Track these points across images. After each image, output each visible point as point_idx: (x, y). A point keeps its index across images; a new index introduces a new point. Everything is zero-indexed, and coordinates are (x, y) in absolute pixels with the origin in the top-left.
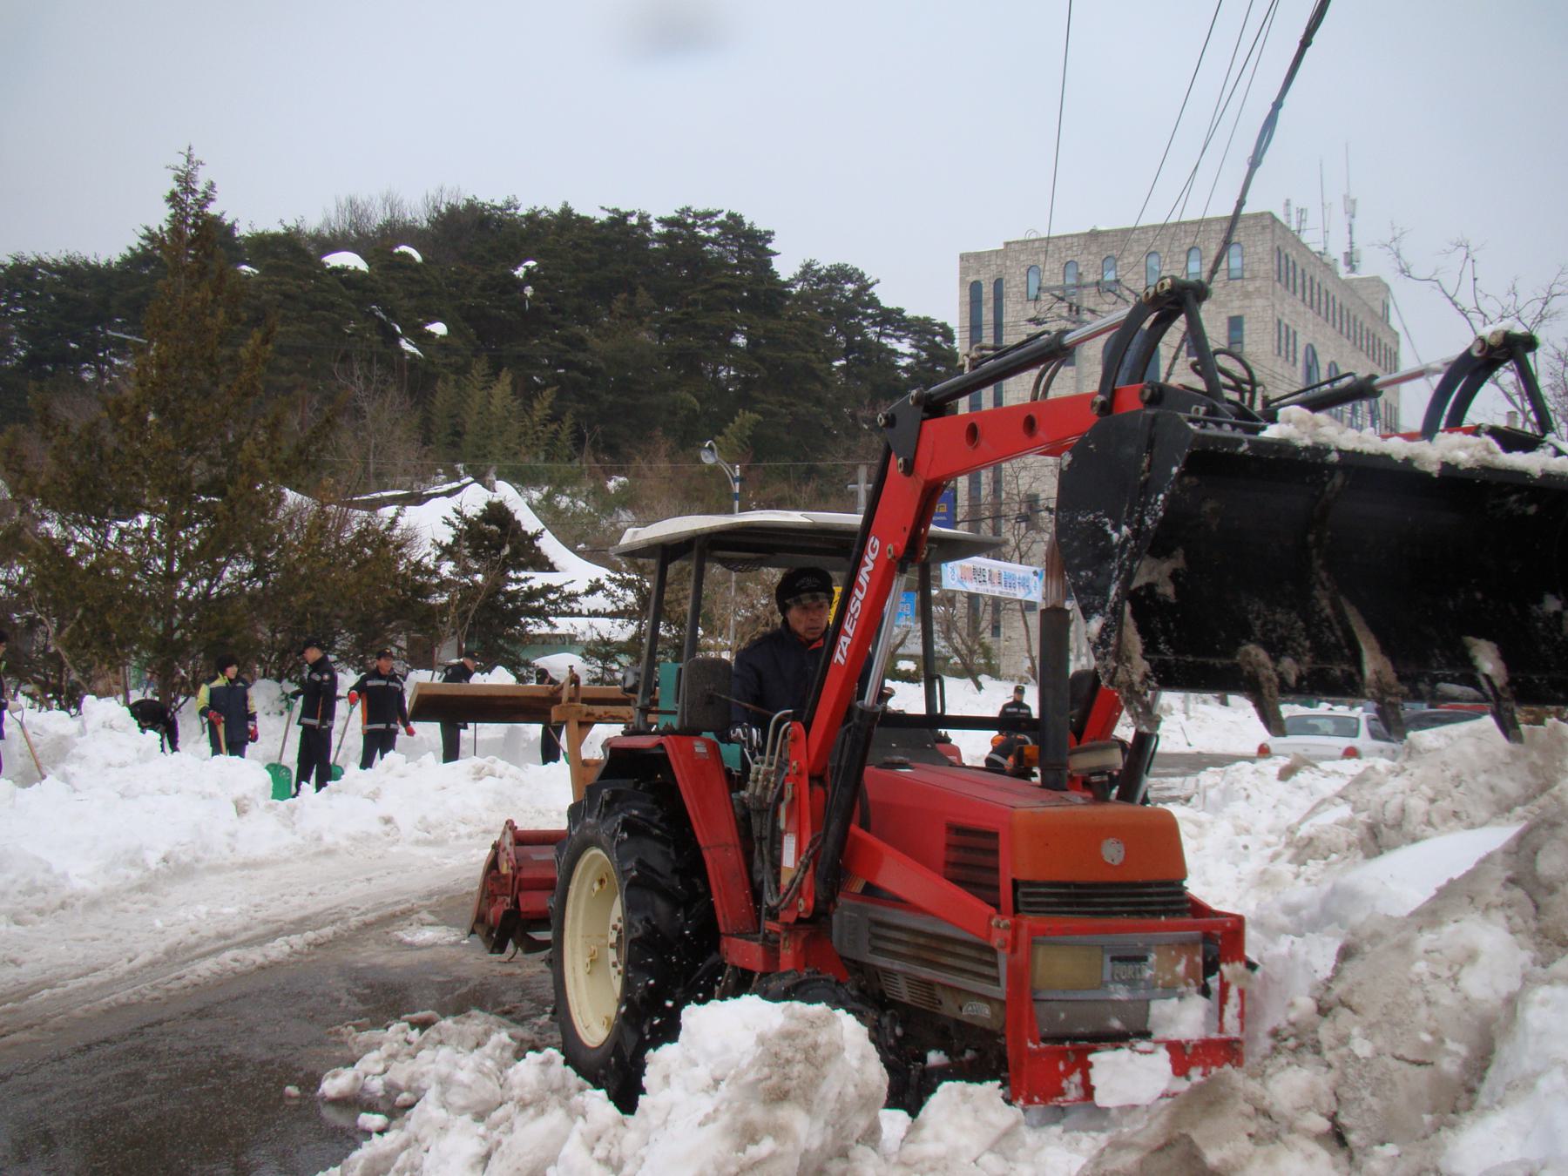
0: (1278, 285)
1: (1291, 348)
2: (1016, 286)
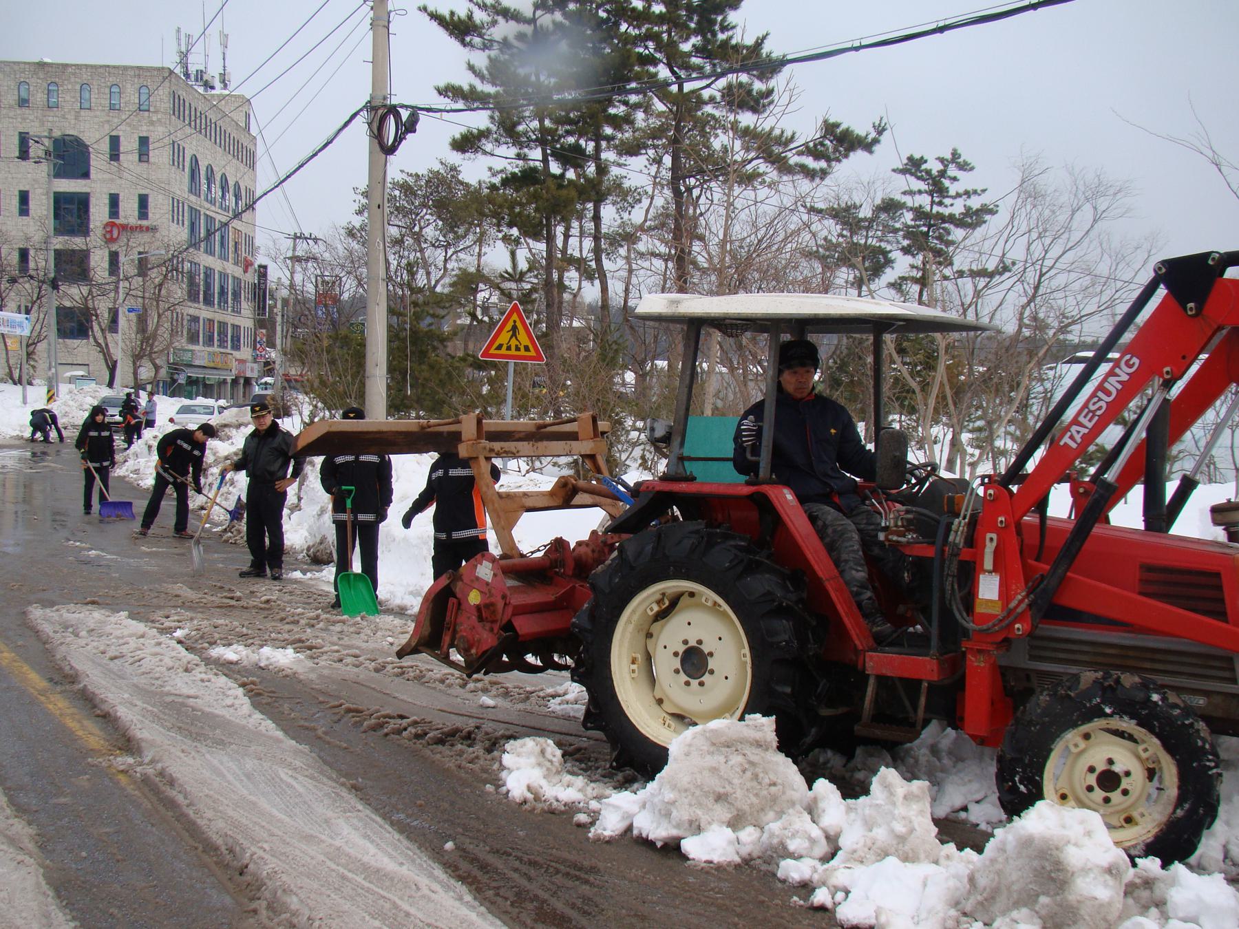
0: (173, 117)
1: (181, 159)
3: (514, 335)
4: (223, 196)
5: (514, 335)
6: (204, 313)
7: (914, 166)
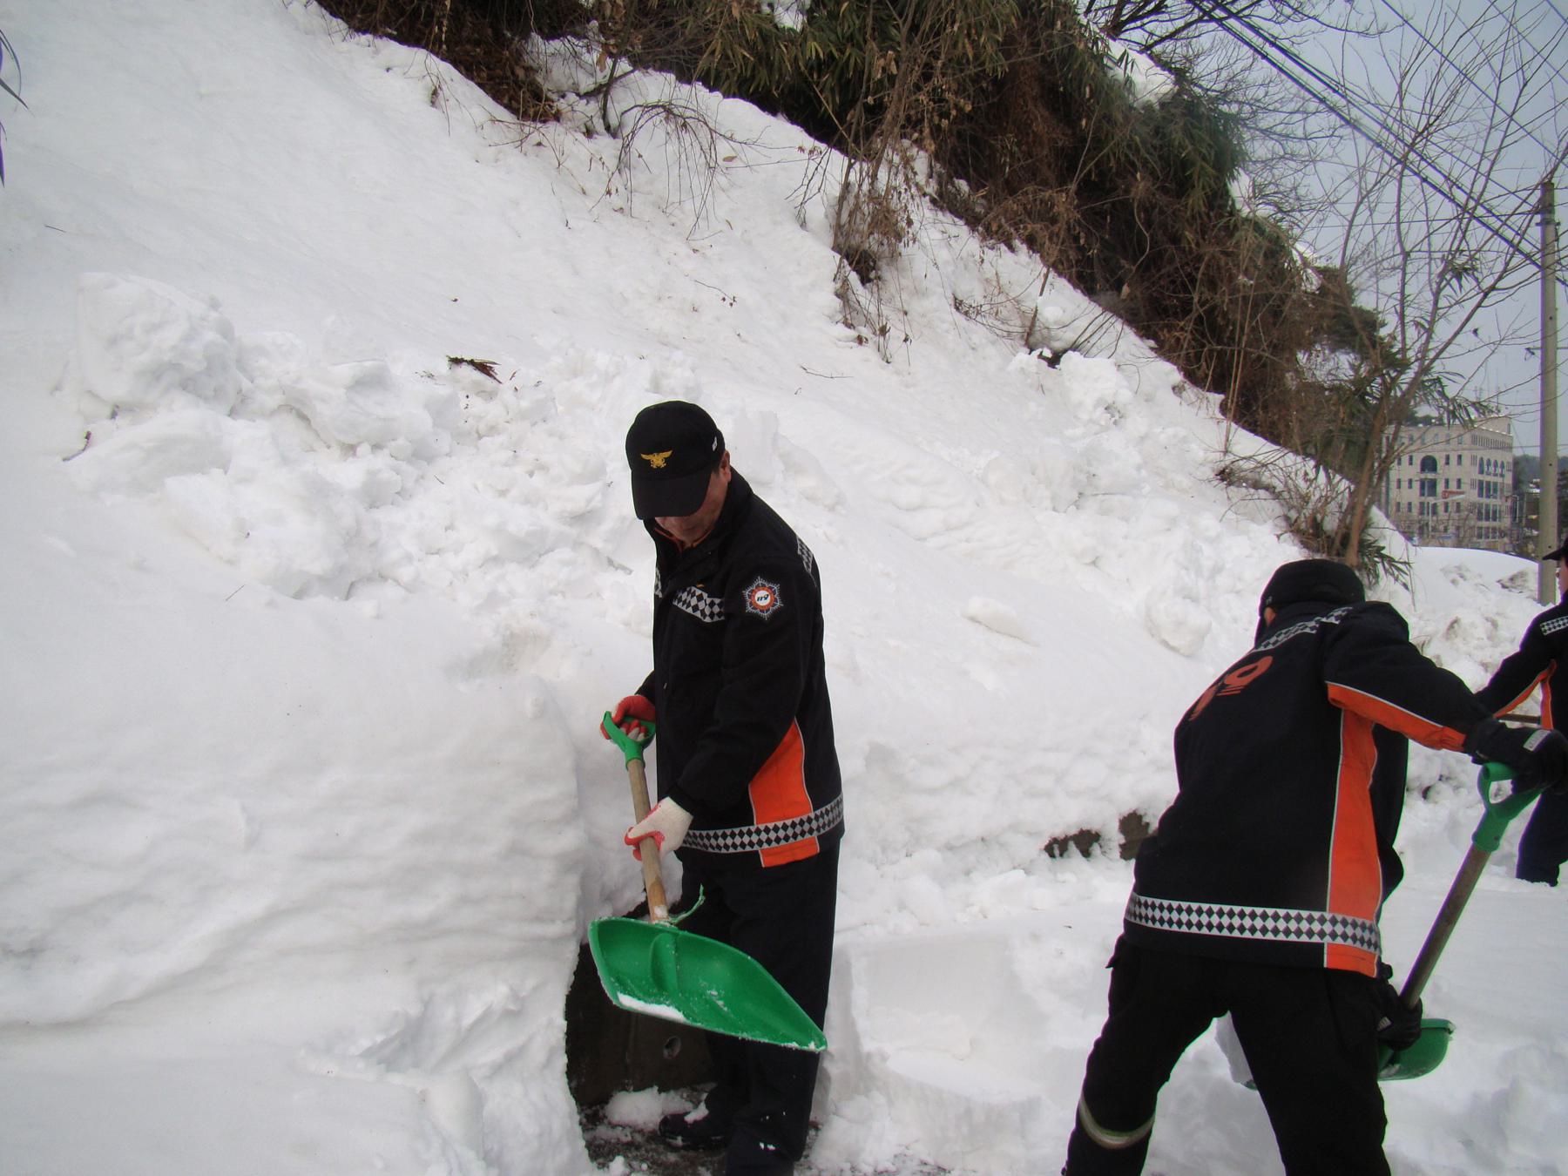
4: (1495, 470)
6: (1484, 524)
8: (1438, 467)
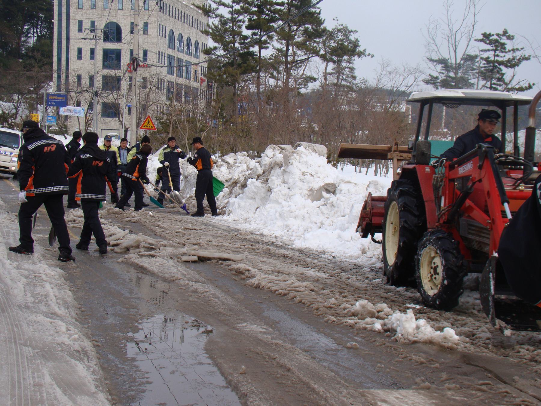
0: (160, 13)
1: (164, 32)
2: (75, 3)
3: (148, 123)
4: (188, 48)
5: (148, 123)
7: (486, 37)
8: (123, 36)
